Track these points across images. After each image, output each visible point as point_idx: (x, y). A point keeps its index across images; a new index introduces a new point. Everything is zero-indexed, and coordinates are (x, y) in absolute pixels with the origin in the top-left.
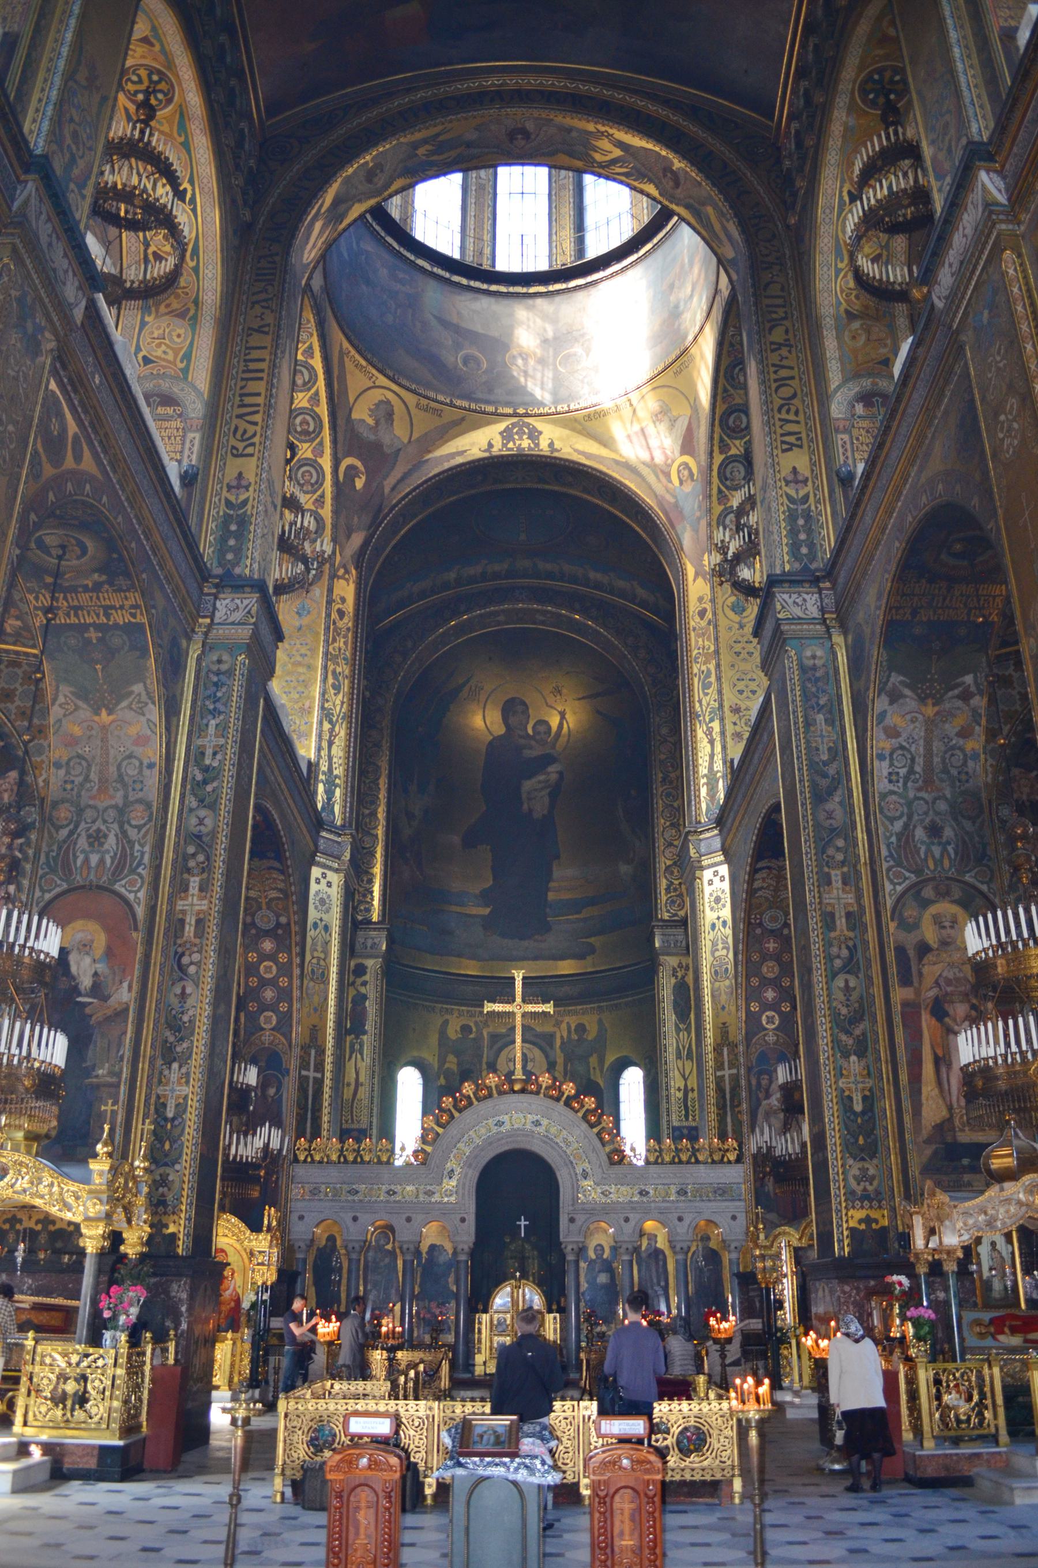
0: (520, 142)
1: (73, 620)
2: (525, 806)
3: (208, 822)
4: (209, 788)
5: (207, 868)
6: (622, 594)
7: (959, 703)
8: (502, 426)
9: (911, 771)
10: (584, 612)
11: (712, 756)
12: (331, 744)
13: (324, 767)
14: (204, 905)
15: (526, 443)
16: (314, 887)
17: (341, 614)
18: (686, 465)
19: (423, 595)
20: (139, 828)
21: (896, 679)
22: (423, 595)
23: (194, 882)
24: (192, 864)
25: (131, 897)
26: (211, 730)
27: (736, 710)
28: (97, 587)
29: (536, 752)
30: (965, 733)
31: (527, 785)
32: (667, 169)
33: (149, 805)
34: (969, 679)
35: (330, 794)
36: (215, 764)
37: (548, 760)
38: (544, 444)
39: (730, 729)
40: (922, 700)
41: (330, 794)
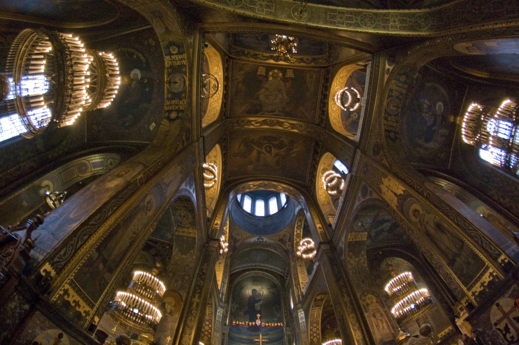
0: (266, 186)
1: (182, 235)
2: (256, 308)
3: (202, 283)
4: (203, 277)
5: (200, 293)
6: (275, 270)
7: (362, 257)
8: (257, 238)
9: (356, 272)
10: (268, 273)
11: (298, 292)
12: (223, 287)
13: (222, 291)
14: (198, 300)
15: (261, 240)
16: (218, 314)
17: (227, 265)
18: (289, 244)
19: (240, 268)
20: (187, 280)
21: (351, 254)
22: (240, 268)
23: (197, 296)
24: (197, 291)
25: (182, 294)
26: (205, 265)
27: (302, 283)
28: (188, 228)
29: (257, 299)
30: (364, 263)
31: (256, 305)
32: (290, 190)
33: (190, 276)
34: (363, 252)
35: (222, 296)
36: (205, 272)
37: (260, 300)
38: (264, 241)
39: (301, 287)
40: (356, 258)
41: (222, 296)
